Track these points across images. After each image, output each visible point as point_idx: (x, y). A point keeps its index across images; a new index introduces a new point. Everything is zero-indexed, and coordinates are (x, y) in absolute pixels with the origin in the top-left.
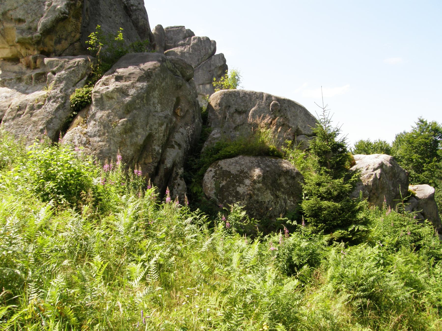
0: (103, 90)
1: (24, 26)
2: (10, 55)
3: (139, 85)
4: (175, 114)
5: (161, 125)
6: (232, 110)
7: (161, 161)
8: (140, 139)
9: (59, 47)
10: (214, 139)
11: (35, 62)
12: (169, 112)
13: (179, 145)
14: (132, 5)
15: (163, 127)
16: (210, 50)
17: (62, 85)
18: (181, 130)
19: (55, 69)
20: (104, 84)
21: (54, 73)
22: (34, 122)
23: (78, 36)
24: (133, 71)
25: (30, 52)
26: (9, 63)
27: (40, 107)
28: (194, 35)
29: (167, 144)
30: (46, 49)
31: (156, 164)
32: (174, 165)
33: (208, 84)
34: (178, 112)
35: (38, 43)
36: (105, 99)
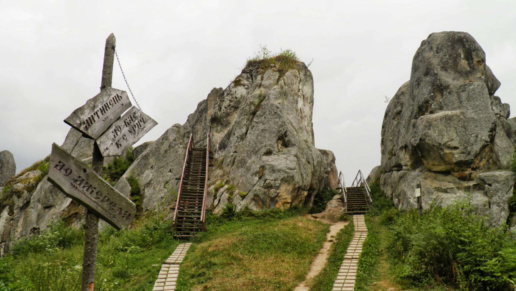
2: (444, 170)
19: (490, 182)
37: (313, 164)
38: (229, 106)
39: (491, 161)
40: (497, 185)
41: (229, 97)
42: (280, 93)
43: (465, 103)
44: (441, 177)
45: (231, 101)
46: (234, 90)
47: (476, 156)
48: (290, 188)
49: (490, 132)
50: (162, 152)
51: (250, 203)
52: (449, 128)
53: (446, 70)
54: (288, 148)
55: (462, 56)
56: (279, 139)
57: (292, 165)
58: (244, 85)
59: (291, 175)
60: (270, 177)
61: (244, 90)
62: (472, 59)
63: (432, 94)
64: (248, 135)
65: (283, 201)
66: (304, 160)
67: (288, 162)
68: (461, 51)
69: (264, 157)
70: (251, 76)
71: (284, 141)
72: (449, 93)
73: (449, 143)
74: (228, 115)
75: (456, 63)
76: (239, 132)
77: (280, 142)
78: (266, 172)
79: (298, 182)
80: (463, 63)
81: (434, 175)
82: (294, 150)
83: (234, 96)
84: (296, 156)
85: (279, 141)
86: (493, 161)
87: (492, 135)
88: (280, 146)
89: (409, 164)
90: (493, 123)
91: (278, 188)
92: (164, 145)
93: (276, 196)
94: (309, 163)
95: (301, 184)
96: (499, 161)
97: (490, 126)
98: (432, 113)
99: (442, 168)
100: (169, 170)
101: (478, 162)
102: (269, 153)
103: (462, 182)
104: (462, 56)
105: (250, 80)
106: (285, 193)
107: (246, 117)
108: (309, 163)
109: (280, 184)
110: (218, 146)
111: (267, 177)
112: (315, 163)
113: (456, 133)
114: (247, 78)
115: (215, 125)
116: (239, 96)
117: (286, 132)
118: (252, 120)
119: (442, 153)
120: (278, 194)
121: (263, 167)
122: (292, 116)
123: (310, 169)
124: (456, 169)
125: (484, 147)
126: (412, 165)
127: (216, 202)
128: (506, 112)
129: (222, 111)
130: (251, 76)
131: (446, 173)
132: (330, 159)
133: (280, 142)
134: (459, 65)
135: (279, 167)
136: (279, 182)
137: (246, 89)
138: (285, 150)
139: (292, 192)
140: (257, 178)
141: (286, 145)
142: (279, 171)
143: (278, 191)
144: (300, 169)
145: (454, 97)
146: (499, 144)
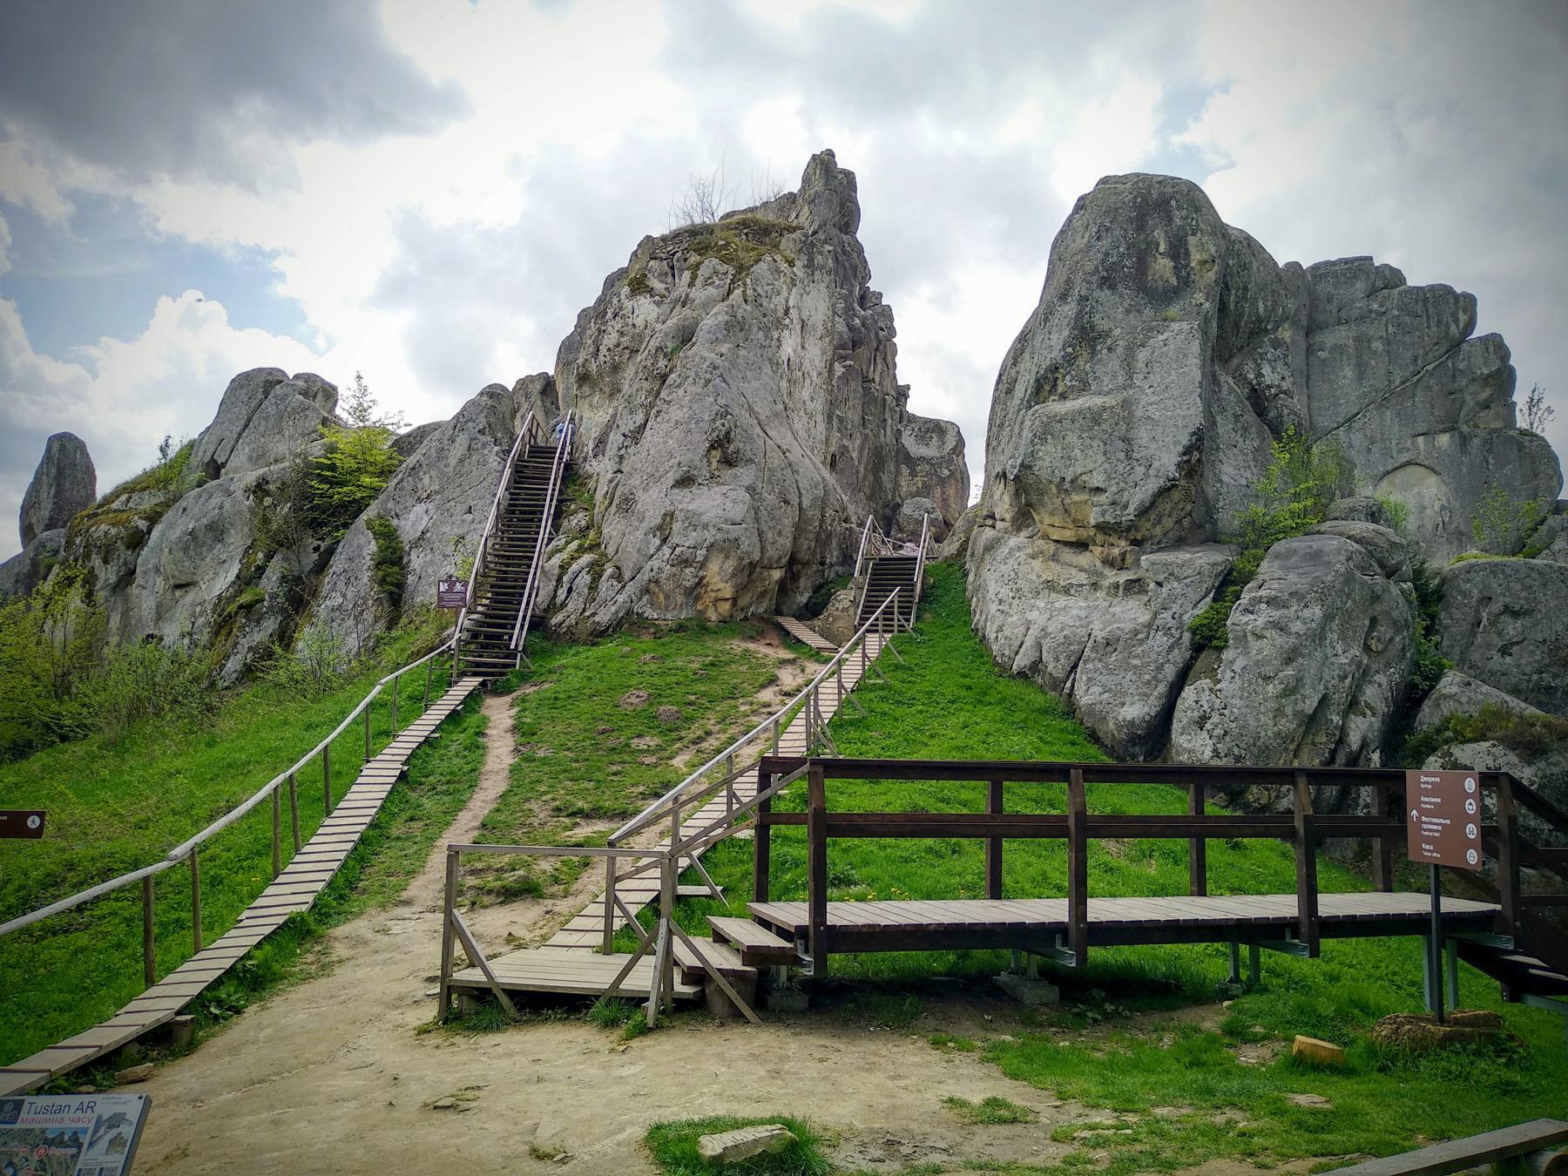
0: (1247, 623)
1: (1102, 498)
3: (1307, 613)
4: (1367, 648)
6: (1496, 607)
7: (1341, 741)
8: (1310, 705)
9: (1158, 530)
10: (1446, 697)
12: (1356, 651)
13: (1371, 708)
14: (1269, 387)
15: (1348, 681)
16: (1453, 327)
17: (1175, 607)
18: (1377, 678)
19: (1161, 578)
20: (1247, 611)
22: (1135, 667)
24: (1294, 589)
25: (1111, 540)
26: (1067, 549)
27: (1142, 642)
28: (1403, 280)
29: (1352, 705)
30: (1139, 537)
32: (1364, 744)
33: (1444, 431)
34: (1374, 644)
35: (1128, 530)
36: (1250, 639)
37: (800, 504)
38: (618, 345)
39: (1186, 522)
41: (618, 324)
42: (728, 327)
43: (1138, 380)
44: (1068, 555)
45: (622, 334)
46: (628, 304)
47: (1143, 512)
48: (730, 565)
50: (453, 461)
52: (1088, 442)
53: (1113, 287)
54: (734, 470)
55: (1162, 249)
56: (712, 447)
57: (737, 512)
58: (651, 291)
60: (684, 539)
61: (653, 306)
62: (1187, 254)
63: (1070, 350)
64: (648, 432)
65: (713, 595)
66: (771, 499)
67: (729, 505)
69: (676, 491)
70: (672, 268)
72: (1110, 349)
73: (1084, 478)
74: (616, 368)
75: (1142, 265)
76: (628, 424)
77: (717, 454)
78: (676, 526)
79: (749, 554)
80: (1162, 266)
81: (1052, 547)
82: (746, 474)
83: (630, 321)
84: (750, 489)
85: (714, 453)
86: (1193, 522)
87: (1188, 461)
88: (715, 464)
89: (1008, 517)
90: (1194, 434)
91: (703, 565)
92: (457, 444)
93: (698, 584)
94: (786, 502)
95: (756, 556)
96: (1215, 523)
97: (1185, 440)
98: (1063, 397)
99: (1068, 535)
100: (466, 507)
101: (1148, 525)
102: (685, 481)
103: (1107, 571)
105: (670, 279)
106: (717, 578)
107: (646, 385)
108: (786, 502)
109: (706, 558)
110: (591, 446)
111: (675, 539)
112: (806, 503)
113: (1105, 453)
114: (662, 276)
115: (586, 390)
116: (639, 322)
117: (728, 433)
118: (658, 393)
119: (1067, 501)
120: (702, 578)
121: (669, 516)
122: (756, 384)
123: (789, 519)
124: (1100, 538)
125: (1163, 492)
126: (1014, 520)
128: (1463, 318)
129: (602, 358)
130: (672, 268)
131: (1081, 545)
132: (951, 443)
133: (717, 454)
134: (1151, 272)
135: (705, 518)
136: (704, 551)
138: (728, 473)
139: (734, 575)
140: (657, 542)
141: (728, 462)
142: (706, 526)
143: (701, 573)
144: (757, 520)
145: (1114, 363)
146: (1225, 479)
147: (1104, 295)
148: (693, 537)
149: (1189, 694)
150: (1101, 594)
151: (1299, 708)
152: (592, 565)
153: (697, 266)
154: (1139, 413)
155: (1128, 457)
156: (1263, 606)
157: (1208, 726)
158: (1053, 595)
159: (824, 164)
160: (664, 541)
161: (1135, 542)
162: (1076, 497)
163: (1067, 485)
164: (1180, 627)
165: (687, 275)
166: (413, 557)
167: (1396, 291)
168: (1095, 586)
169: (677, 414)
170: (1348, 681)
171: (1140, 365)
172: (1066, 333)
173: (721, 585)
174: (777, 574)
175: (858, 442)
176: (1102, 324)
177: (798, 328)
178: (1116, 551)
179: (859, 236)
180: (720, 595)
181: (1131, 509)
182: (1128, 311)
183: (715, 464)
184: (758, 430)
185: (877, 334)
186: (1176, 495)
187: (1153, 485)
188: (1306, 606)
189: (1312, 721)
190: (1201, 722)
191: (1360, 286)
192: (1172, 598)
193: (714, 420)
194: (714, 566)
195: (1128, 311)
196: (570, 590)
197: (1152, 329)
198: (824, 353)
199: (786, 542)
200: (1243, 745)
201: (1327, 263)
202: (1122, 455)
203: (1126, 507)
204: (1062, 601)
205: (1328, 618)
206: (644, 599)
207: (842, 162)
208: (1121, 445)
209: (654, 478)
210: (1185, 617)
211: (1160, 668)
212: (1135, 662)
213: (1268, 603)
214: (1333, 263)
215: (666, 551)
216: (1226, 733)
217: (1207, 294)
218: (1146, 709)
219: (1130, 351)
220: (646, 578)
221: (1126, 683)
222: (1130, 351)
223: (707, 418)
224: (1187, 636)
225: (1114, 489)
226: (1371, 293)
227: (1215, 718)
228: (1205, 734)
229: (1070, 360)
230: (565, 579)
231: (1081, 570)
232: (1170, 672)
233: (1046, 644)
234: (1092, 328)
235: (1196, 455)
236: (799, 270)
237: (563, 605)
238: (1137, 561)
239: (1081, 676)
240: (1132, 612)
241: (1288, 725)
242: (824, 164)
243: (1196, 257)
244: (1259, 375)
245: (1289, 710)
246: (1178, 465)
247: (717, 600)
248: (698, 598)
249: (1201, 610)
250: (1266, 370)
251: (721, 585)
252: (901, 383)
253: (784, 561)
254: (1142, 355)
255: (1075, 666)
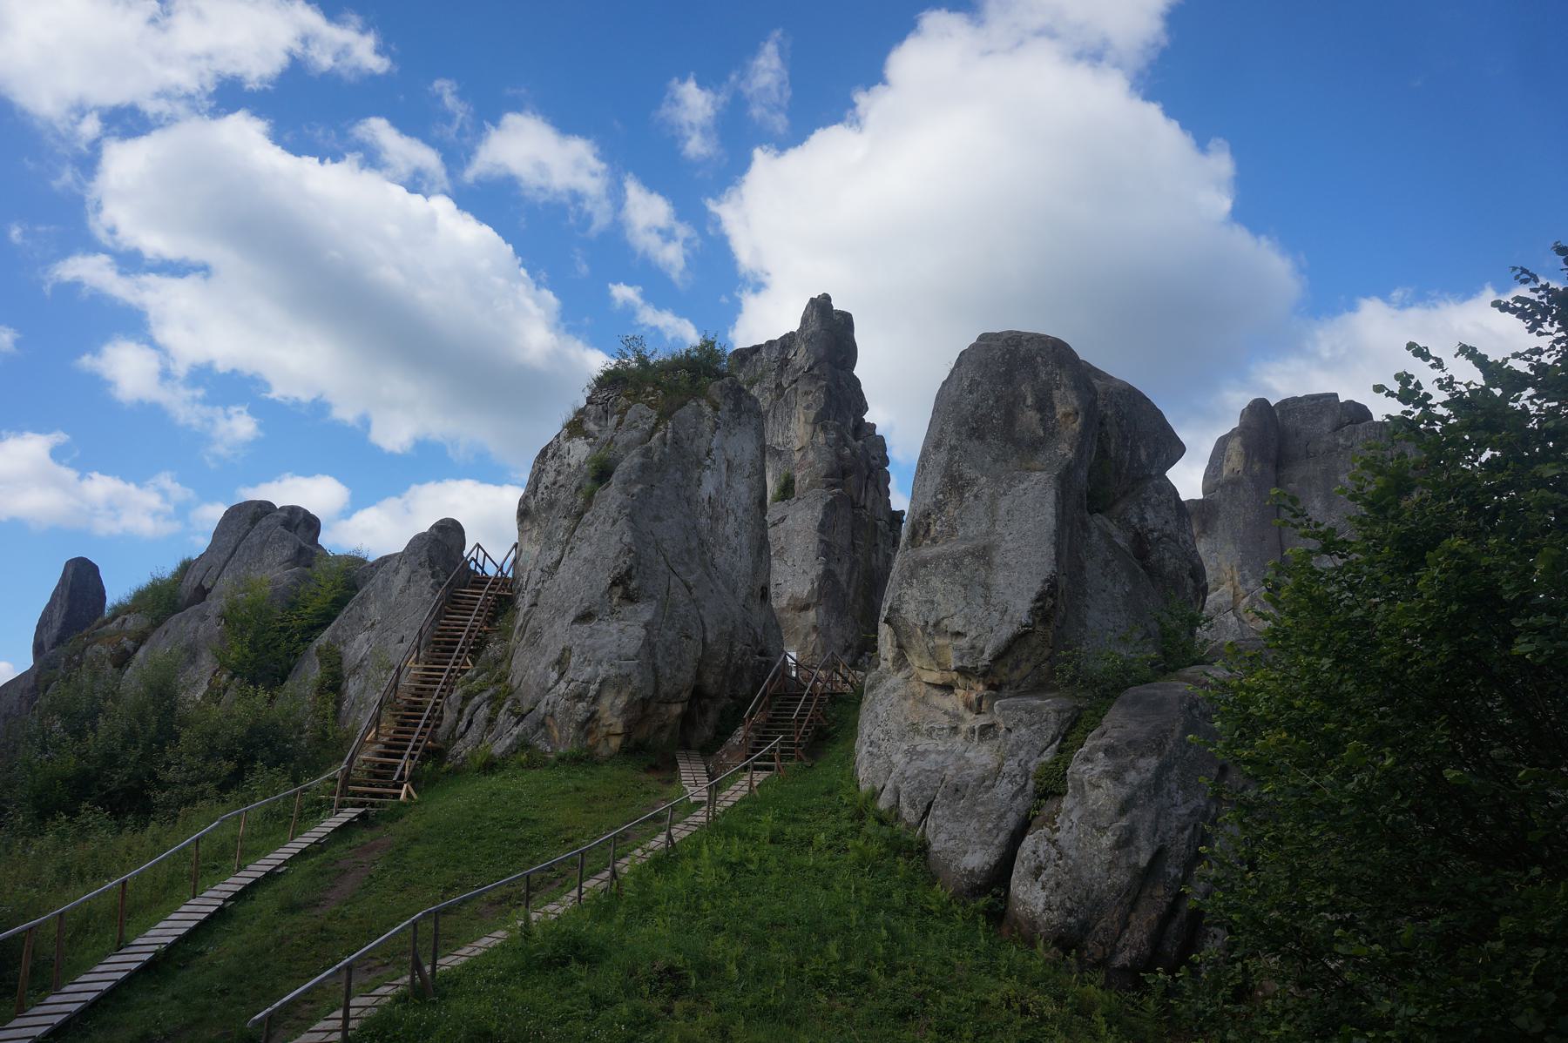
1: (964, 643)
3: (1142, 763)
5: (1182, 830)
7: (1180, 897)
8: (1143, 859)
9: (1016, 675)
11: (980, 705)
14: (1152, 531)
17: (1022, 754)
20: (1087, 760)
21: (1009, 730)
22: (980, 814)
23: (1047, 652)
26: (935, 692)
27: (988, 788)
28: (1368, 415)
31: (1170, 900)
35: (984, 674)
37: (704, 639)
40: (1023, 731)
44: (937, 698)
45: (559, 473)
47: (999, 657)
48: (621, 702)
49: (1037, 600)
50: (395, 592)
51: (535, 732)
53: (981, 438)
55: (1029, 401)
56: (614, 584)
58: (587, 435)
59: (624, 671)
62: (1053, 408)
63: (940, 496)
64: (561, 568)
68: (1026, 389)
71: (626, 589)
72: (976, 497)
75: (1010, 417)
77: (619, 590)
81: (924, 688)
82: (646, 611)
85: (615, 589)
88: (615, 600)
89: (890, 656)
91: (596, 699)
95: (649, 692)
97: (1037, 586)
99: (935, 677)
102: (585, 617)
104: (1029, 401)
109: (599, 693)
111: (570, 675)
112: (710, 637)
116: (573, 462)
121: (567, 651)
127: (462, 725)
131: (948, 688)
133: (619, 590)
137: (590, 445)
139: (624, 711)
140: (554, 675)
141: (629, 598)
146: (1090, 623)
147: (973, 445)
148: (589, 670)
149: (1029, 842)
150: (960, 738)
151: (1133, 860)
152: (492, 698)
153: (623, 413)
154: (997, 560)
155: (987, 603)
156: (1101, 755)
157: (1043, 878)
158: (917, 738)
159: (821, 307)
160: (561, 675)
161: (991, 687)
162: (939, 641)
163: (930, 630)
164: (1026, 774)
165: (615, 418)
166: (351, 684)
167: (1360, 426)
168: (955, 730)
169: (586, 551)
170: (1187, 833)
171: (1002, 512)
172: (938, 480)
173: (614, 720)
174: (677, 709)
175: (846, 566)
176: (970, 473)
177: (724, 467)
178: (973, 696)
179: (856, 372)
180: (612, 729)
181: (986, 655)
182: (995, 461)
183: (615, 600)
184: (663, 566)
185: (868, 463)
186: (1034, 641)
187: (1006, 632)
188: (1142, 756)
189: (1149, 874)
190: (1037, 872)
191: (1327, 422)
192: (1019, 745)
193: (617, 557)
194: (606, 701)
195: (995, 461)
196: (470, 723)
197: (1013, 478)
198: (751, 490)
199: (686, 677)
200: (1075, 898)
201: (1295, 399)
202: (981, 601)
203: (982, 652)
204: (923, 743)
205: (1163, 769)
206: (540, 733)
207: (837, 305)
208: (980, 590)
209: (561, 612)
210: (1031, 764)
211: (1001, 817)
212: (981, 809)
213: (1106, 752)
214: (1300, 400)
215: (563, 685)
216: (1058, 885)
217: (1071, 445)
218: (987, 858)
219: (994, 498)
220: (543, 711)
221: (970, 830)
222: (994, 498)
223: (611, 555)
224: (1031, 783)
225: (973, 633)
226: (1338, 428)
227: (1050, 870)
228: (1039, 885)
229: (940, 506)
230: (467, 711)
231: (946, 713)
232: (1011, 821)
233: (904, 787)
234: (961, 476)
235: (1050, 601)
236: (724, 413)
237: (462, 735)
238: (991, 707)
239: (931, 822)
240: (982, 756)
241: (1122, 878)
242: (821, 307)
243: (1060, 410)
244: (1143, 519)
245: (1123, 862)
246: (1032, 612)
247: (609, 735)
248: (589, 733)
249: (1047, 757)
250: (1150, 515)
251: (614, 720)
252: (895, 507)
253: (685, 695)
254: (1004, 504)
255: (926, 814)
